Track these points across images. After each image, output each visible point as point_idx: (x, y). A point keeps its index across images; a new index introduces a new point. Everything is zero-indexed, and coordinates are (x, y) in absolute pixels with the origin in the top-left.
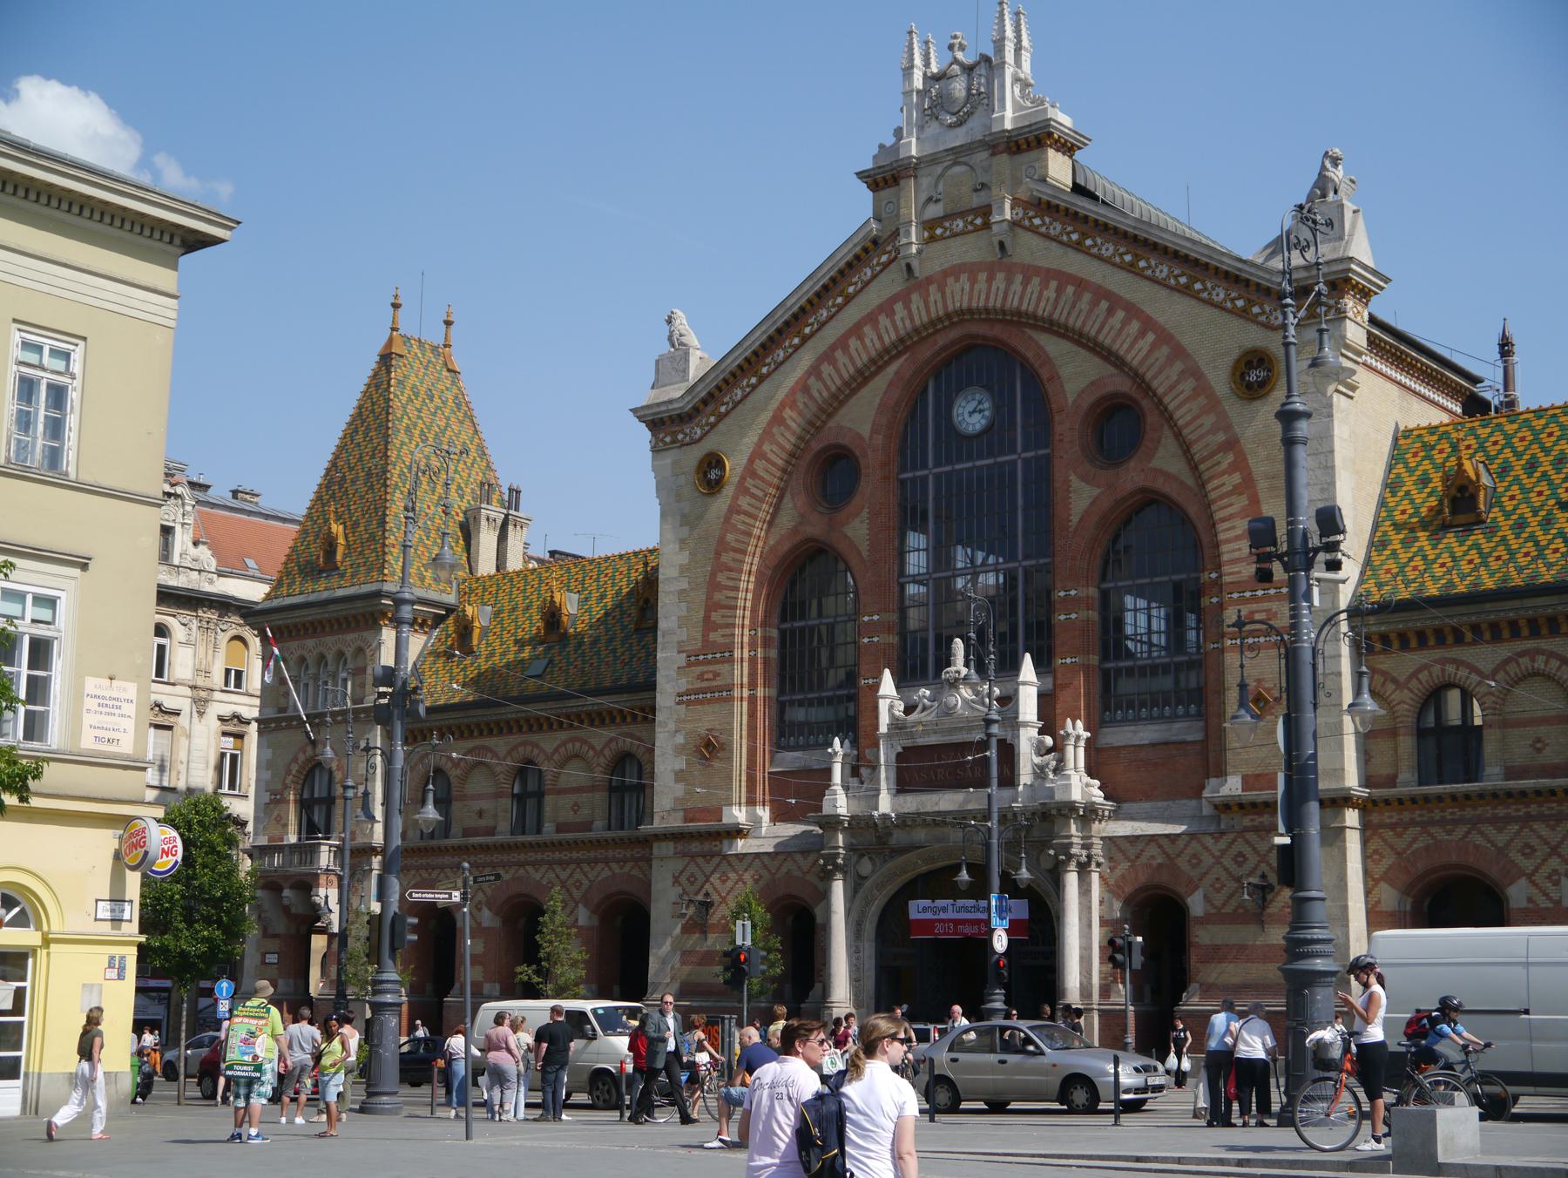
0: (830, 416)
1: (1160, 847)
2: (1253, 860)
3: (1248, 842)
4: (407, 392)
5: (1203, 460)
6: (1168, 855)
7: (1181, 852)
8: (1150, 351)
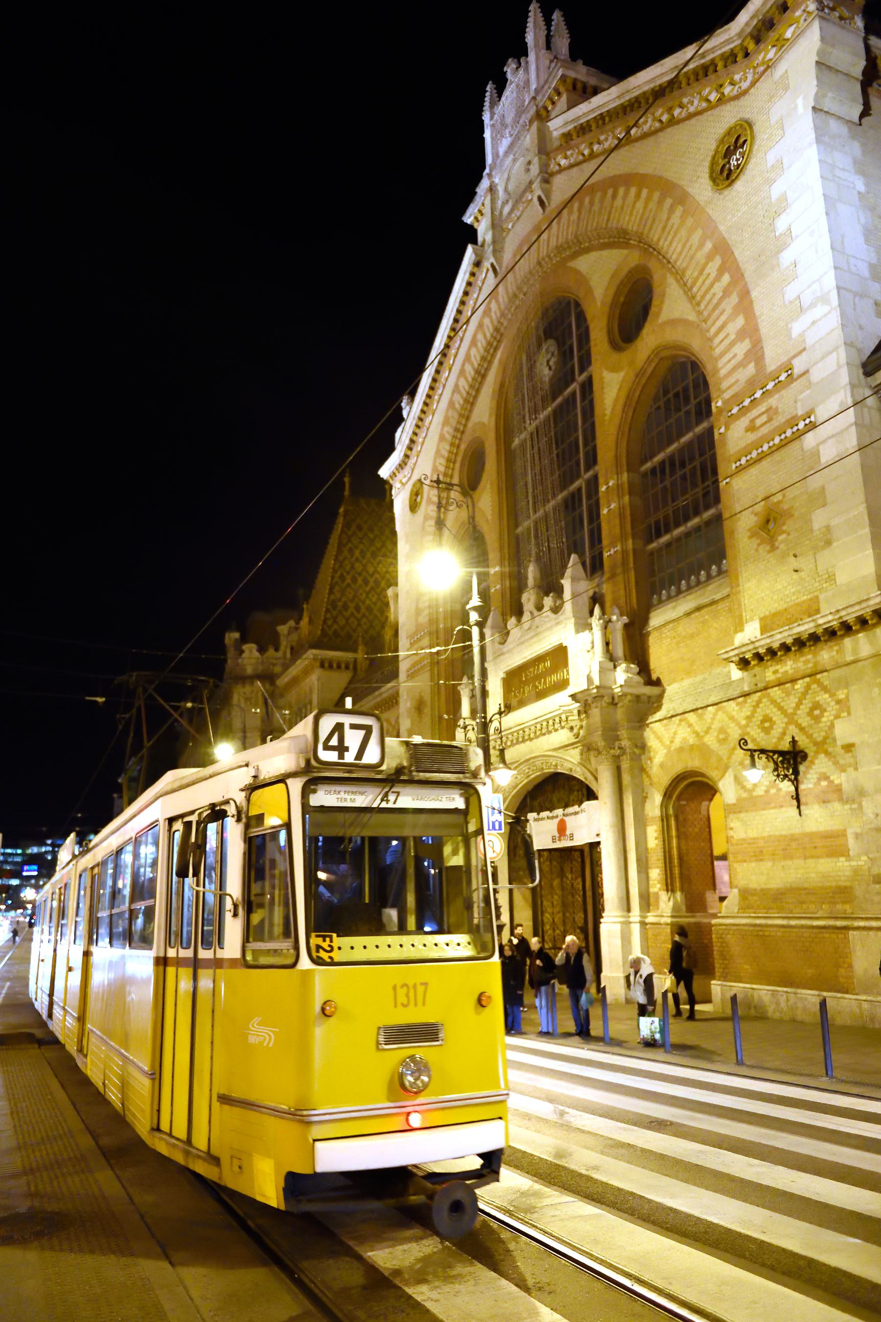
0: (468, 419)
1: (690, 725)
2: (780, 721)
3: (773, 702)
4: (353, 528)
5: (694, 283)
6: (697, 734)
7: (709, 728)
8: (645, 207)
